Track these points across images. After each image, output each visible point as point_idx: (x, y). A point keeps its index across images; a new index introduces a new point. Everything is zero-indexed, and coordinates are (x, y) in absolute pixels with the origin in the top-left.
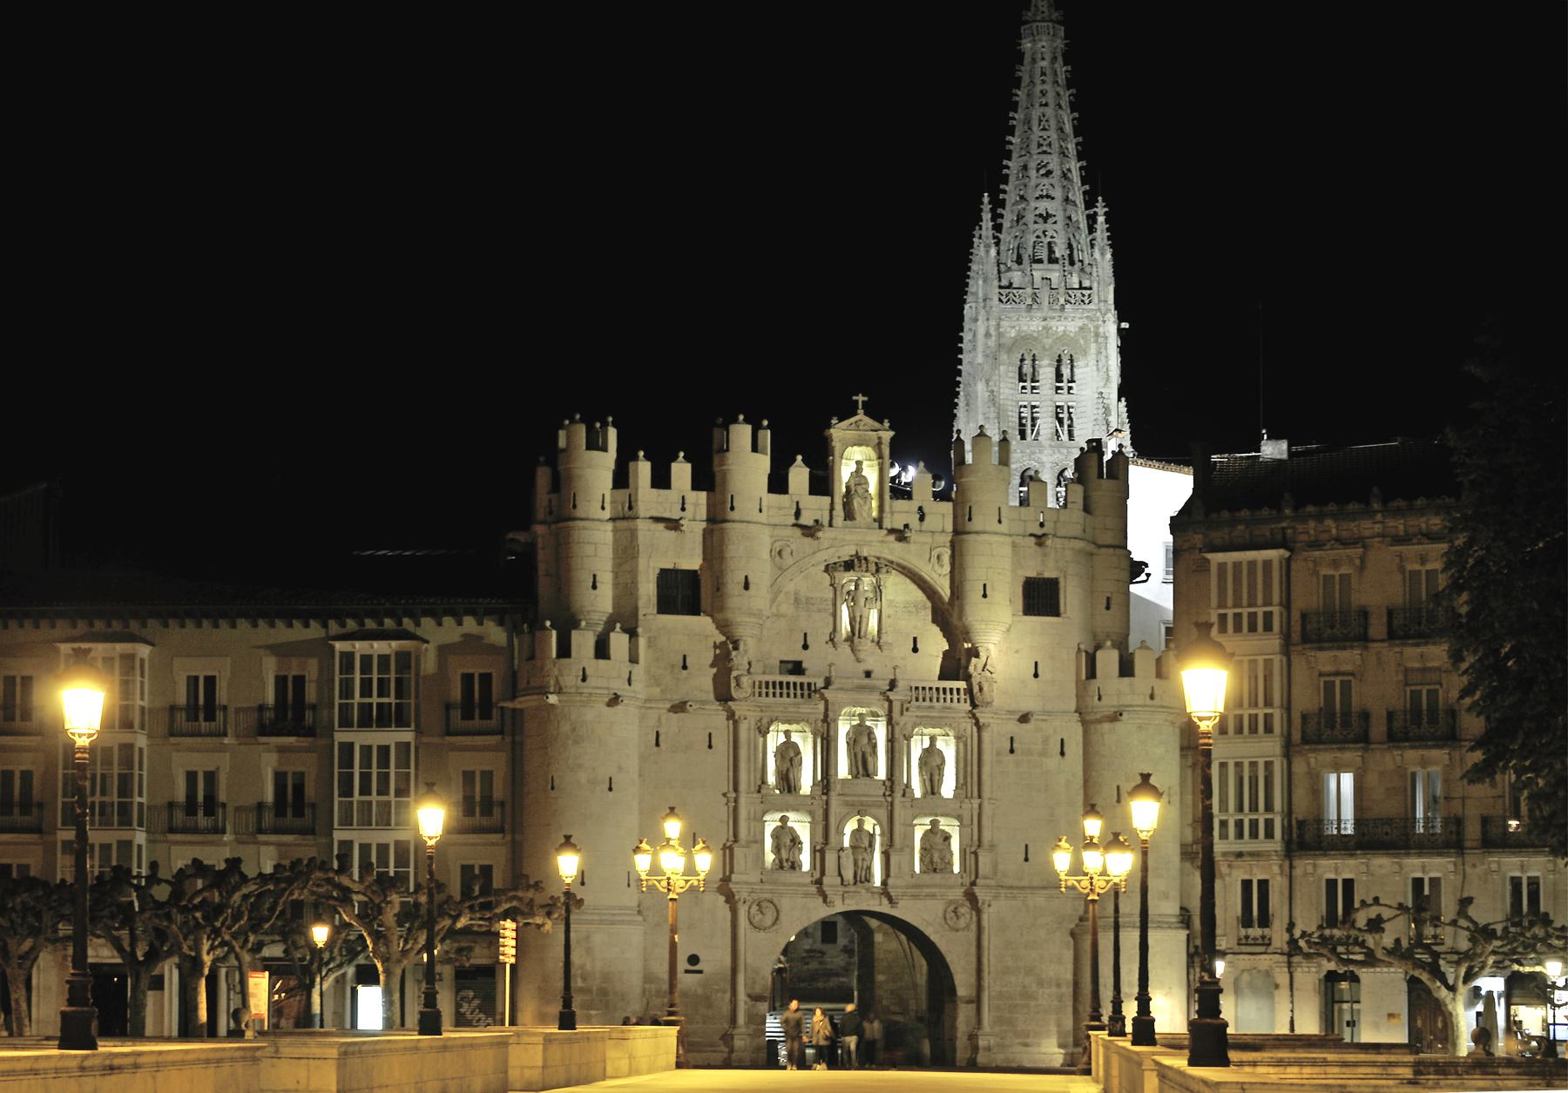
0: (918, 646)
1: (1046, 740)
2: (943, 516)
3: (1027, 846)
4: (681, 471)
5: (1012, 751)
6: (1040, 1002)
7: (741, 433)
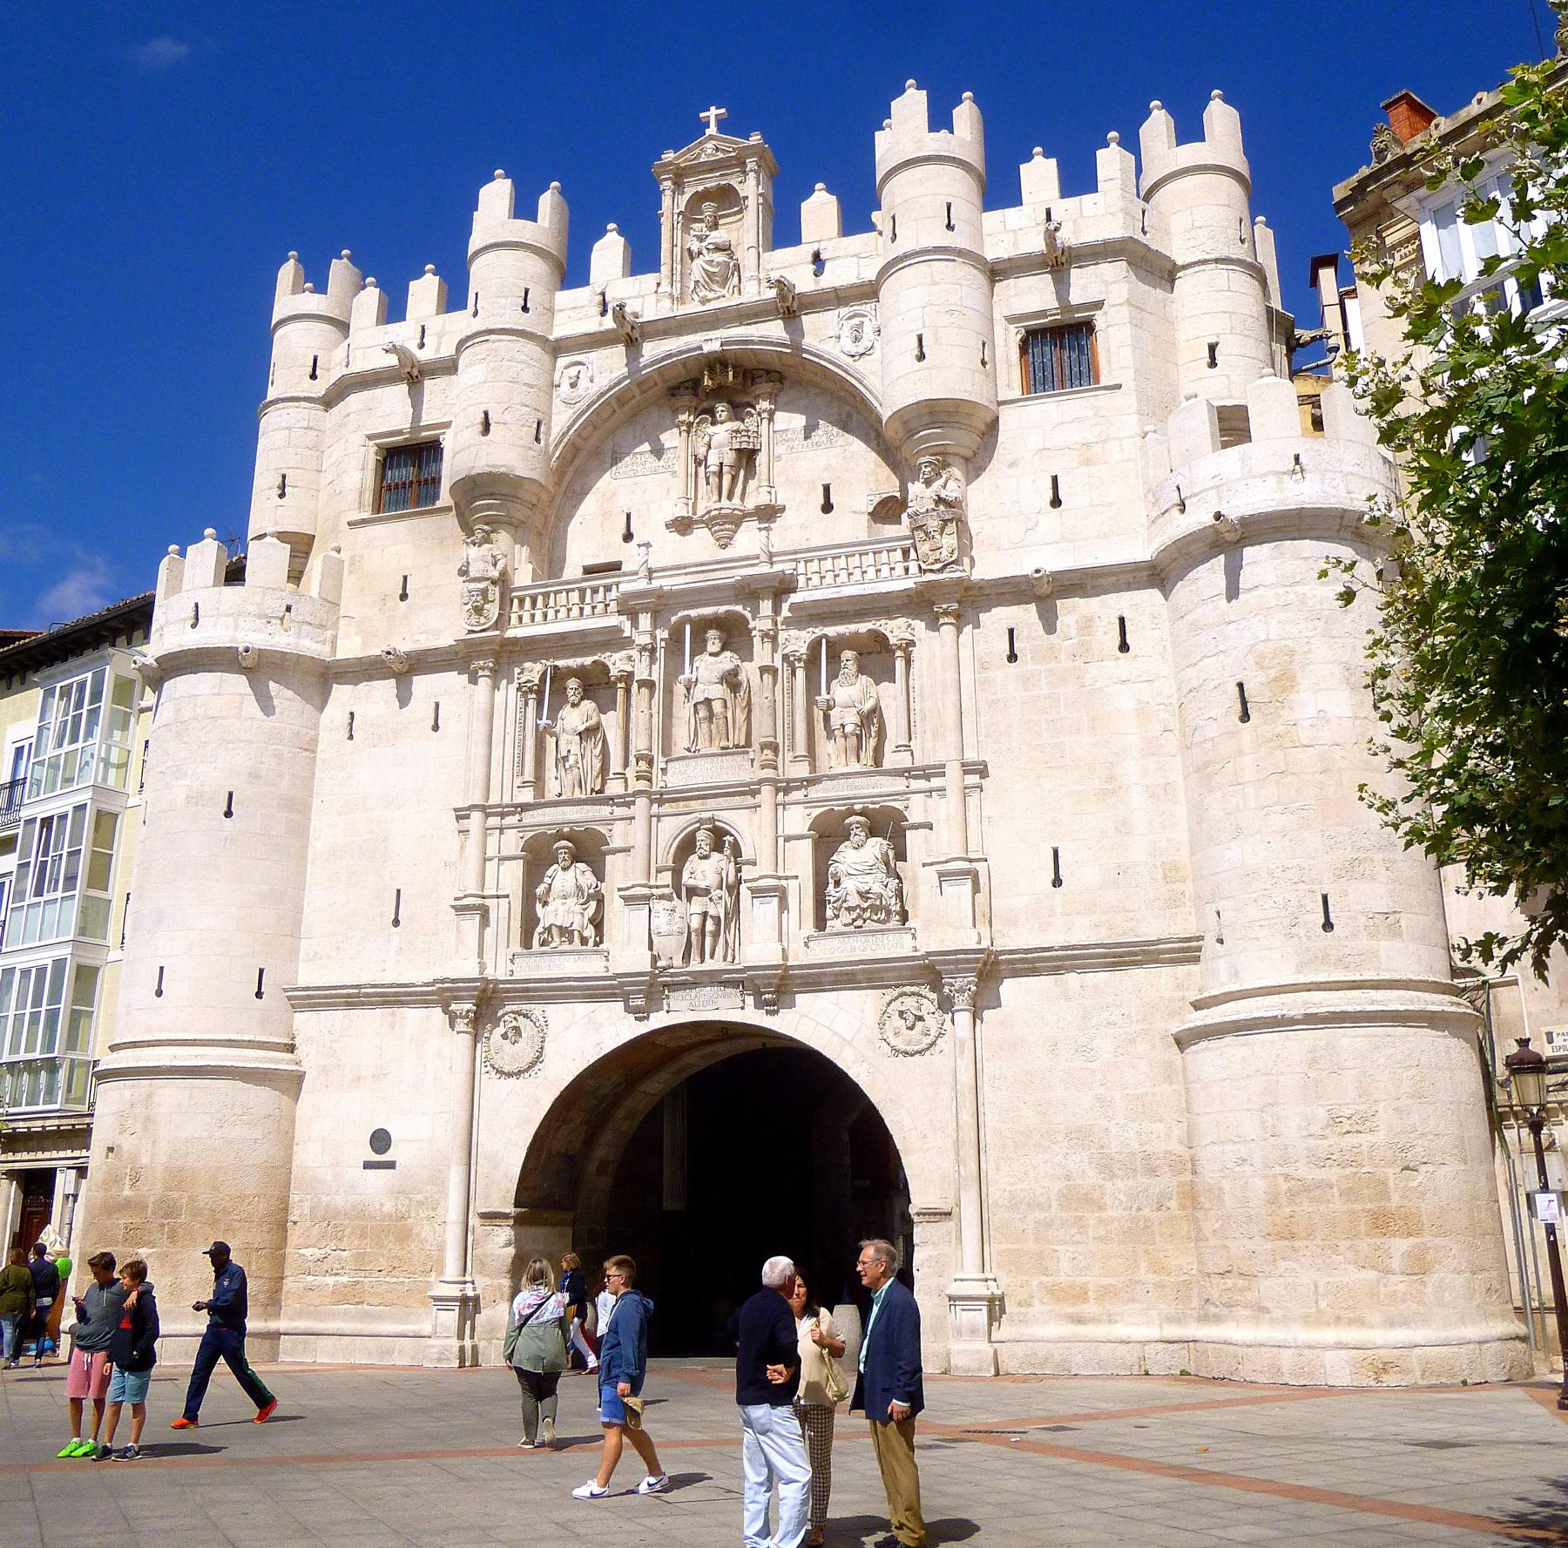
0: (832, 500)
1: (1087, 625)
4: (425, 290)
5: (1012, 657)
6: (1110, 1213)
7: (496, 195)
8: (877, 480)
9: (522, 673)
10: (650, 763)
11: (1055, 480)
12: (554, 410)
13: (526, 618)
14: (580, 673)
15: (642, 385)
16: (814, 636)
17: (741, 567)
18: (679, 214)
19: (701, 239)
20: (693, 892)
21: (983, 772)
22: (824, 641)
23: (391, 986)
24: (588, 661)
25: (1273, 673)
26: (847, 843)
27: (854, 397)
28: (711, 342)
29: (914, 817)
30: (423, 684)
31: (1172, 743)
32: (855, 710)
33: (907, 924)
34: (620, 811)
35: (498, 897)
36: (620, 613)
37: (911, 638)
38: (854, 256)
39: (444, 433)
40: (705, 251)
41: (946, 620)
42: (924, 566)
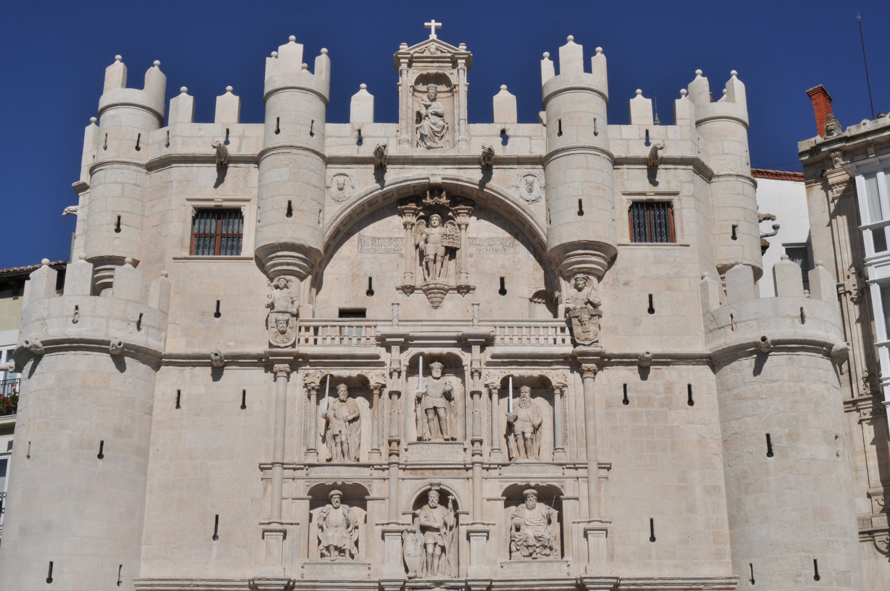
0: (506, 287)
1: (669, 387)
2: (530, 138)
3: (652, 521)
5: (626, 401)
8: (534, 279)
9: (307, 375)
10: (399, 443)
11: (651, 296)
12: (327, 203)
13: (311, 341)
14: (347, 381)
15: (384, 195)
16: (504, 375)
17: (459, 326)
18: (411, 87)
19: (427, 107)
20: (424, 529)
21: (609, 469)
22: (511, 378)
23: (217, 580)
24: (354, 372)
25: (787, 430)
26: (524, 505)
27: (524, 225)
28: (437, 175)
29: (567, 493)
30: (231, 374)
31: (718, 463)
32: (531, 424)
33: (565, 559)
34: (376, 474)
35: (292, 524)
36: (378, 345)
37: (565, 383)
38: (528, 137)
39: (244, 206)
40: (430, 116)
41: (589, 375)
42: (578, 341)
